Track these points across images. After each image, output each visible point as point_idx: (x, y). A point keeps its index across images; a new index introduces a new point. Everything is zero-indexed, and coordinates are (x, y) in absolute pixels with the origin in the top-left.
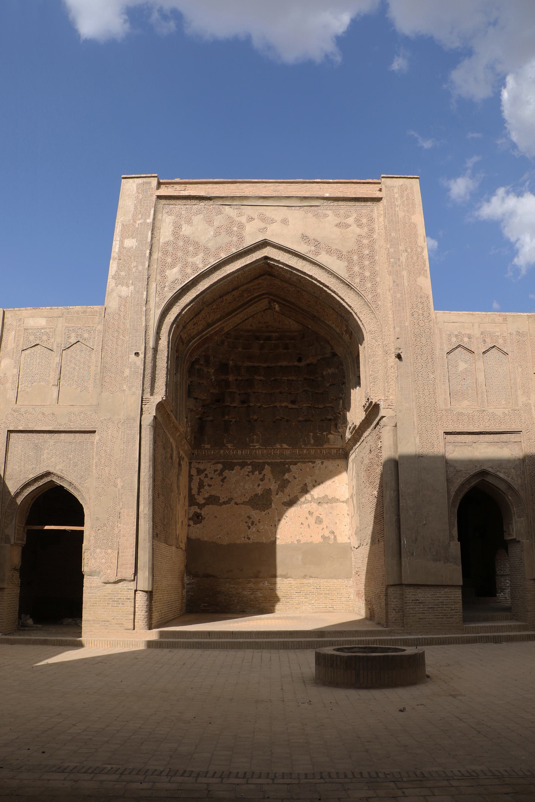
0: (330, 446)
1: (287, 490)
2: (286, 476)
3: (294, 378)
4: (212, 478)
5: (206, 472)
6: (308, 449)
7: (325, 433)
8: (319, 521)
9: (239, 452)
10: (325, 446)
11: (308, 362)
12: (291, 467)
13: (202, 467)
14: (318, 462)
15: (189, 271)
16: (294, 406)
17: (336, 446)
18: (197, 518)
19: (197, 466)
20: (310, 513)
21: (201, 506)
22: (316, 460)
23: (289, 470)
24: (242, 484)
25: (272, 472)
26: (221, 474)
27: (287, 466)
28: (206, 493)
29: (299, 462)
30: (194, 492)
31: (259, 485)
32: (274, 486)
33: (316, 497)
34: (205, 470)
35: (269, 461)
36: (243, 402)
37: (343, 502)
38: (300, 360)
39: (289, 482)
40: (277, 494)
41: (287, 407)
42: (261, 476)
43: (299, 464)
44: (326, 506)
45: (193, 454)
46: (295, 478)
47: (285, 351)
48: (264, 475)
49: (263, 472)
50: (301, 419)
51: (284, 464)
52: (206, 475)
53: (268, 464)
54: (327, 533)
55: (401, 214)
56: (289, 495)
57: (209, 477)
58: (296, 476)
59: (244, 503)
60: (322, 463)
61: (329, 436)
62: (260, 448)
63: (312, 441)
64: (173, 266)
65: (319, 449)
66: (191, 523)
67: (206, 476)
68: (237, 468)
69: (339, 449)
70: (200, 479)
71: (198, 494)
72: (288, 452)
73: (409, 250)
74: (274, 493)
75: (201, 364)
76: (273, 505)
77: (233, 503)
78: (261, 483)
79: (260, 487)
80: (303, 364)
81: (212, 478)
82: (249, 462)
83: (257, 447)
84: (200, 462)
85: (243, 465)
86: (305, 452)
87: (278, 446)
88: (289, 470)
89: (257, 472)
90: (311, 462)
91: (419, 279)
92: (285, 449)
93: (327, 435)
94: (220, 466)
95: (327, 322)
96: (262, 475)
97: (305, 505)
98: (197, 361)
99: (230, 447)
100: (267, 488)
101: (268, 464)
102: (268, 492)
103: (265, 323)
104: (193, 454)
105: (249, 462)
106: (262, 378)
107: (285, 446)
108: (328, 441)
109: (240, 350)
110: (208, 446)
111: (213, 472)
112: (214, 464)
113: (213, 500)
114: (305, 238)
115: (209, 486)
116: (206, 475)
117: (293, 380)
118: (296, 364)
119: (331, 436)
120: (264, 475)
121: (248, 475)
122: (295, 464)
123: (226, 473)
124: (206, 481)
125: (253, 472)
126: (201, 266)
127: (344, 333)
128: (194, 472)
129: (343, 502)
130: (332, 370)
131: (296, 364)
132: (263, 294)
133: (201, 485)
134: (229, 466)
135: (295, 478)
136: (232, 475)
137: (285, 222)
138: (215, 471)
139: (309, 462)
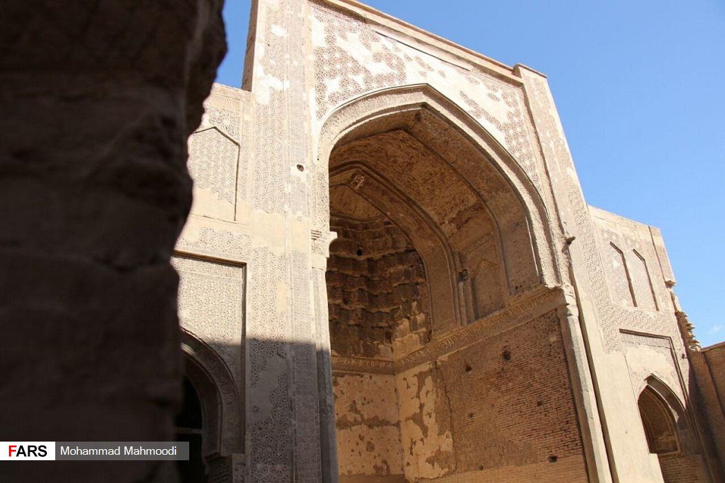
0: (380, 358)
7: (375, 342)
10: (376, 358)
11: (369, 256)
14: (367, 375)
15: (351, 88)
16: (346, 307)
17: (386, 359)
22: (364, 374)
29: (346, 374)
33: (366, 417)
37: (393, 425)
38: (360, 253)
43: (346, 376)
44: (376, 429)
46: (343, 394)
47: (345, 239)
50: (352, 322)
58: (344, 391)
60: (371, 377)
61: (380, 346)
64: (332, 75)
65: (370, 360)
69: (389, 362)
80: (362, 258)
90: (359, 375)
93: (378, 344)
95: (423, 208)
97: (355, 427)
108: (378, 352)
114: (463, 95)
117: (348, 276)
118: (355, 256)
122: (342, 376)
126: (363, 87)
127: (447, 222)
129: (393, 425)
131: (355, 256)
132: (358, 162)
135: (343, 394)
137: (442, 74)
139: (356, 375)
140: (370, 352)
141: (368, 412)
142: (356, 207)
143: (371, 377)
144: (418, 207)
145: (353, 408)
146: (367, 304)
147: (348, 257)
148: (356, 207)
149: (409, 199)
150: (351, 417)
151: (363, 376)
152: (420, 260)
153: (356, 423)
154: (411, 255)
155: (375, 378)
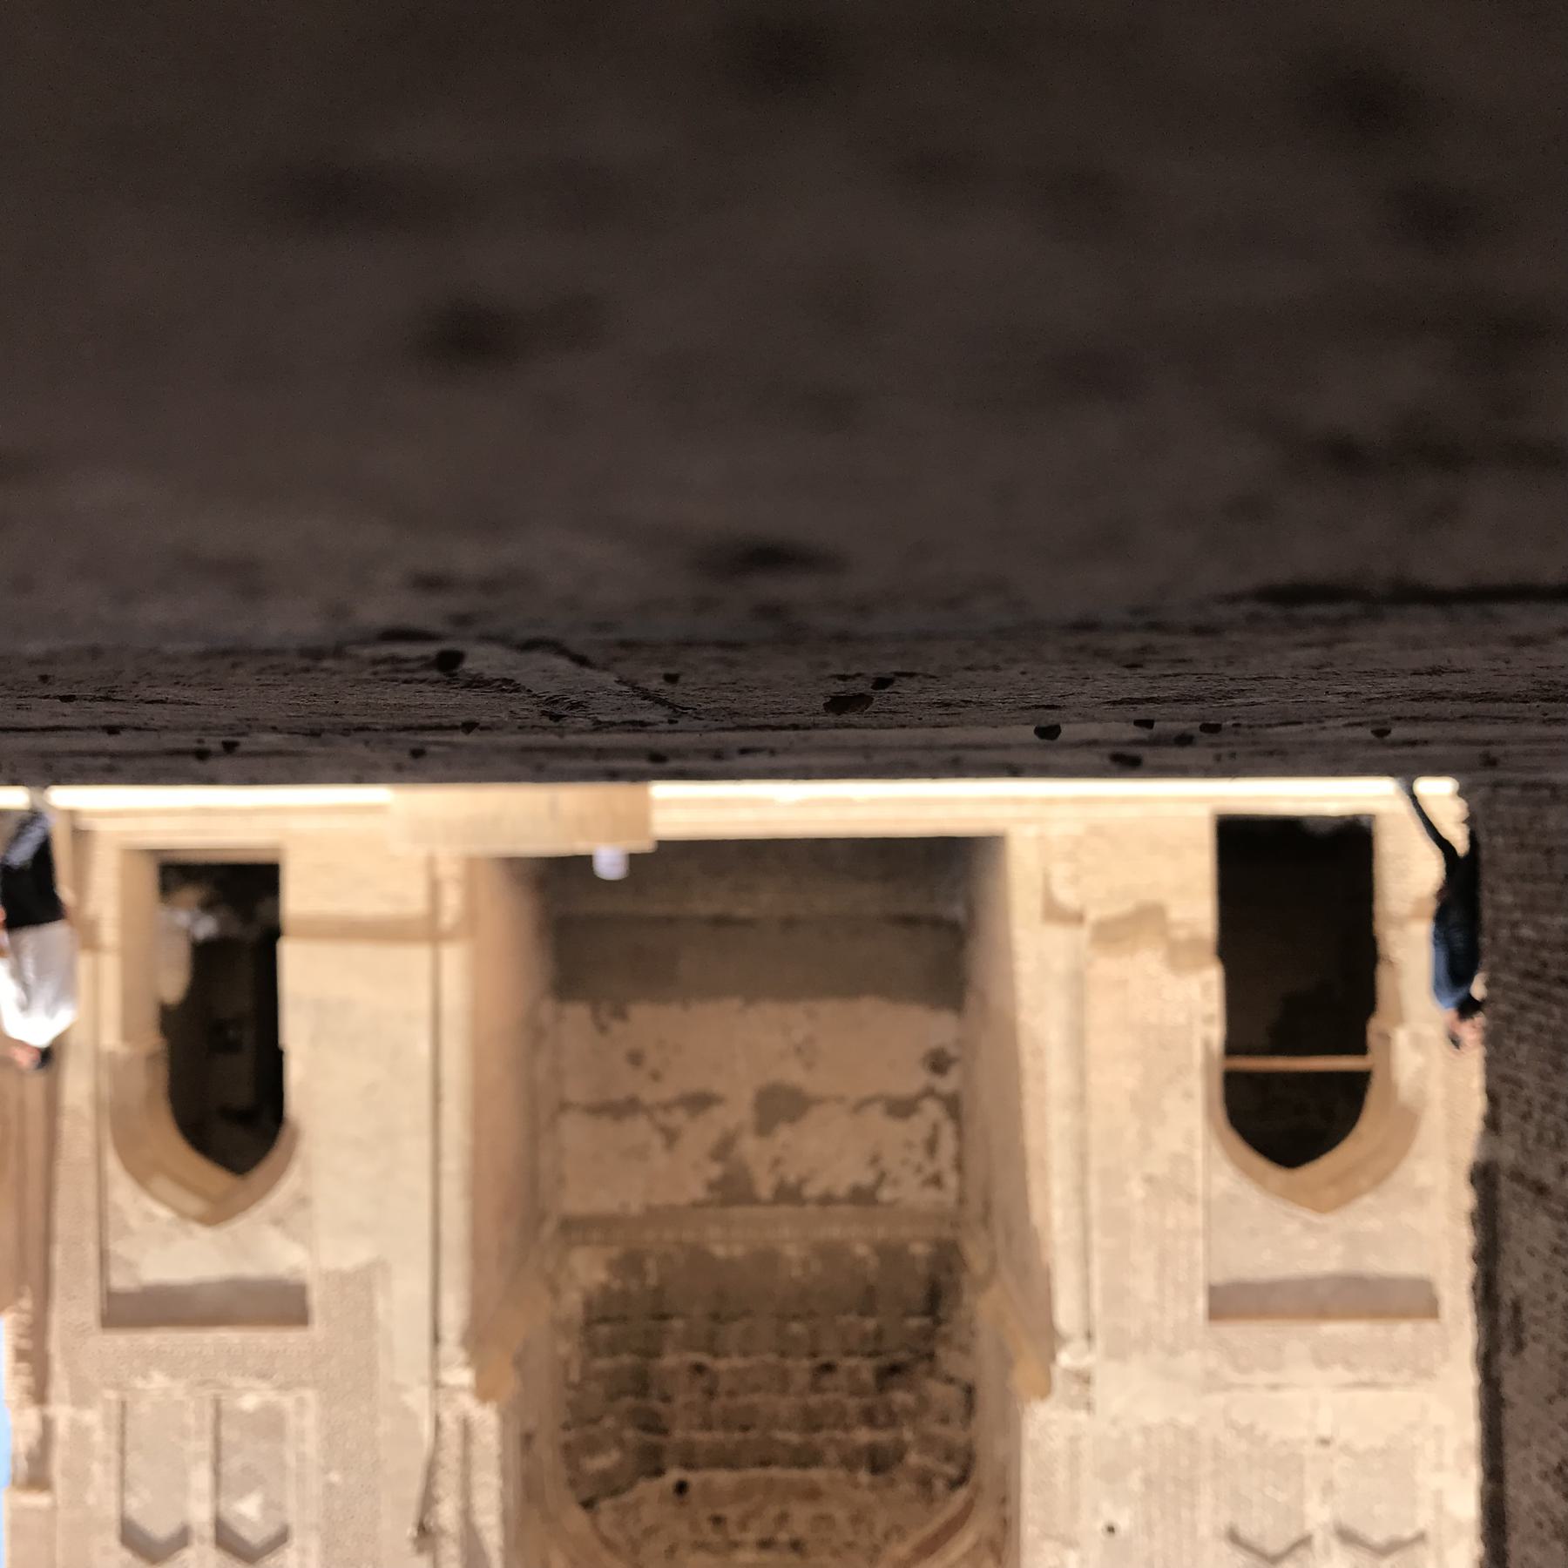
8: (636, 1059)
13: (931, 1194)
18: (939, 1063)
20: (656, 1076)
21: (930, 1092)
23: (712, 1186)
26: (882, 1177)
28: (918, 1127)
30: (947, 1130)
36: (828, 1368)
51: (727, 1202)
54: (617, 1027)
59: (820, 1101)
66: (953, 1051)
67: (919, 1169)
68: (841, 1190)
71: (936, 1127)
72: (714, 1232)
82: (811, 1209)
85: (827, 1200)
88: (712, 1186)
102: (764, 1128)
105: (811, 1209)
106: (780, 1435)
108: (612, 1266)
113: (902, 1108)
115: (909, 1145)
122: (696, 1205)
123: (867, 1178)
124: (918, 1156)
128: (951, 1180)
133: (932, 1146)
134: (862, 1197)
136: (850, 1173)
140: (631, 1263)
141: (639, 1129)
145: (671, 1137)
150: (679, 1117)
153: (667, 1107)
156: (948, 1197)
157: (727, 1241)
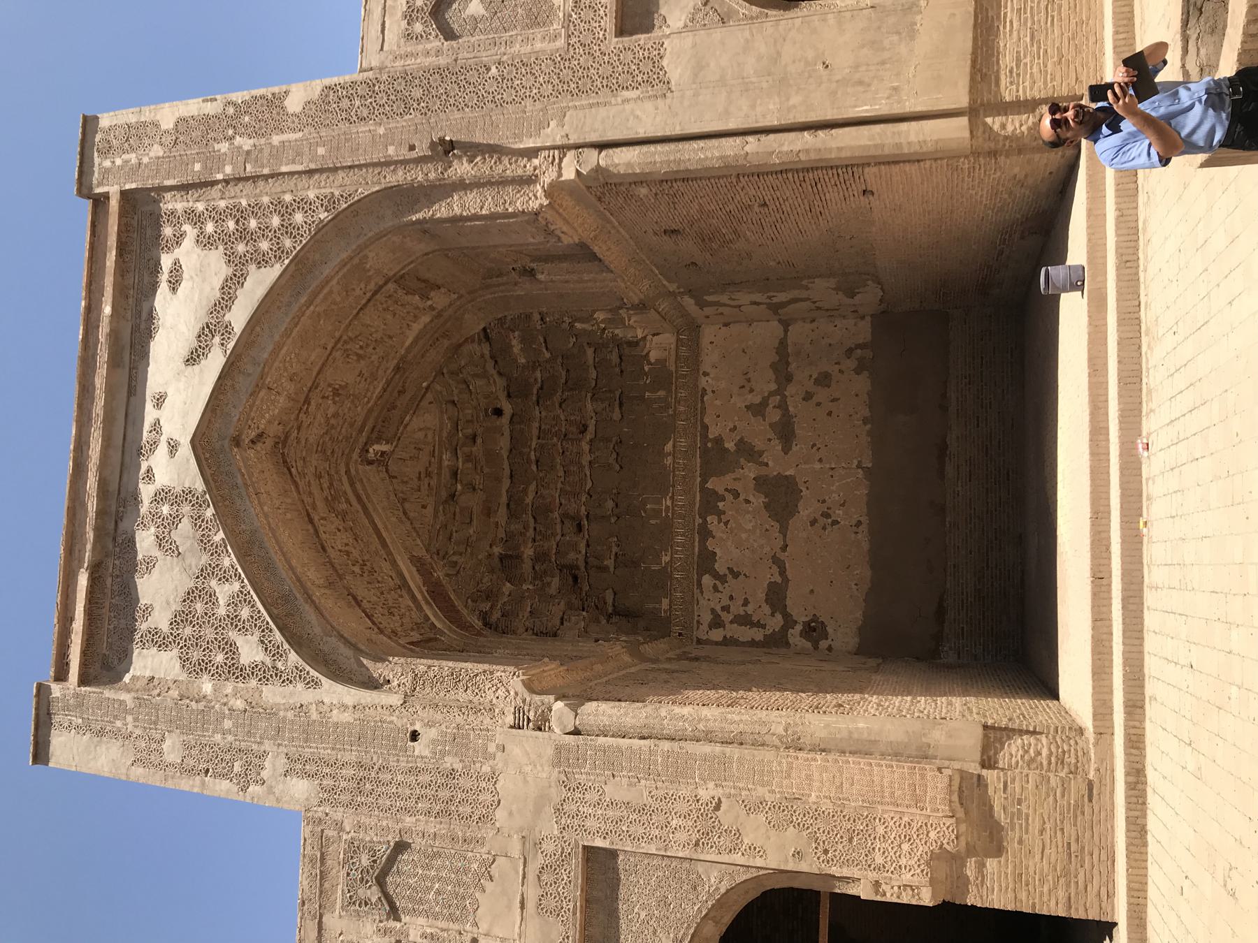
0: (673, 358)
1: (759, 444)
2: (730, 445)
3: (537, 425)
4: (731, 598)
5: (718, 609)
6: (678, 402)
7: (646, 368)
8: (824, 380)
9: (679, 539)
10: (673, 368)
11: (502, 396)
12: (711, 436)
13: (707, 618)
14: (703, 382)
15: (245, 613)
16: (591, 428)
18: (814, 630)
19: (705, 627)
20: (808, 397)
21: (789, 622)
23: (719, 441)
24: (744, 536)
25: (721, 473)
26: (723, 579)
27: (709, 445)
28: (762, 611)
29: (702, 420)
30: (758, 635)
31: (748, 502)
32: (750, 471)
33: (773, 387)
34: (713, 610)
35: (699, 479)
36: (580, 528)
37: (786, 331)
38: (498, 412)
39: (741, 440)
40: (767, 465)
41: (591, 441)
42: (729, 497)
43: (706, 420)
44: (793, 366)
45: (680, 634)
47: (479, 441)
48: (726, 490)
49: (721, 491)
50: (616, 415)
51: (705, 452)
52: (723, 608)
53: (704, 481)
54: (851, 364)
55: (157, 151)
56: (770, 440)
57: (728, 602)
59: (784, 531)
60: (705, 374)
62: (672, 498)
63: (662, 393)
64: (231, 649)
66: (823, 644)
67: (726, 609)
70: (731, 622)
71: (764, 626)
72: (683, 443)
73: (231, 132)
74: (764, 471)
75: (491, 608)
76: (787, 473)
77: (782, 556)
78: (742, 498)
79: (751, 498)
80: (507, 408)
81: (731, 598)
82: (699, 521)
83: (669, 503)
84: (698, 622)
85: (705, 533)
86: (682, 409)
87: (669, 461)
88: (719, 441)
89: (721, 504)
90: (702, 397)
91: (291, 110)
92: (674, 446)
93: (649, 363)
94: (707, 580)
96: (727, 494)
97: (791, 409)
98: (484, 617)
99: (668, 559)
100: (752, 484)
101: (704, 481)
102: (761, 483)
103: (419, 479)
104: (680, 634)
105: (699, 521)
106: (532, 487)
107: (669, 447)
108: (662, 362)
109: (471, 532)
110: (665, 603)
111: (719, 595)
112: (702, 593)
113: (776, 597)
114: (193, 358)
115: (746, 603)
116: (723, 608)
118: (505, 420)
119: (653, 356)
120: (726, 490)
121: (726, 523)
122: (705, 428)
123: (720, 567)
124: (737, 609)
125: (720, 513)
126: (236, 586)
127: (429, 303)
128: (717, 635)
129: (786, 331)
130: (514, 342)
131: (505, 420)
133: (744, 620)
134: (706, 561)
136: (726, 552)
138: (715, 588)
139: (702, 401)
140: (662, 377)
141: (765, 383)
142: (421, 430)
143: (705, 374)
144: (408, 350)
145: (757, 410)
146: (583, 393)
147: (507, 433)
148: (421, 430)
149: (397, 369)
150: (774, 416)
151: (704, 390)
152: (501, 321)
153: (783, 406)
154: (493, 335)
155: (706, 367)
156: (702, 633)
157: (677, 452)
